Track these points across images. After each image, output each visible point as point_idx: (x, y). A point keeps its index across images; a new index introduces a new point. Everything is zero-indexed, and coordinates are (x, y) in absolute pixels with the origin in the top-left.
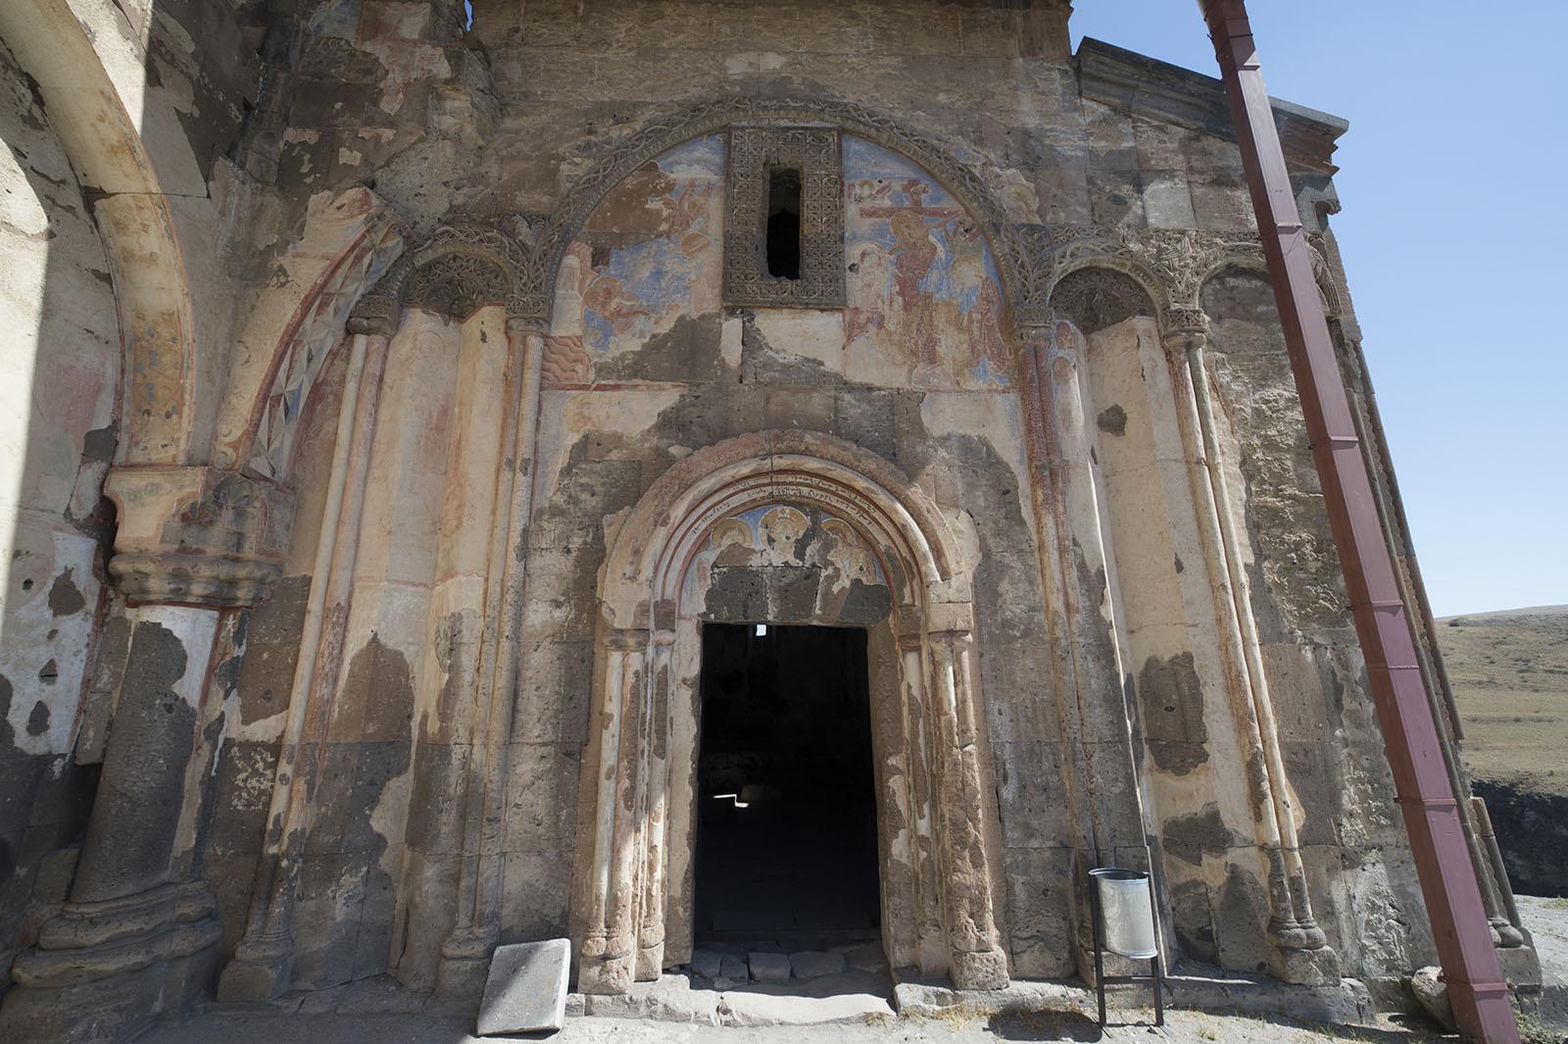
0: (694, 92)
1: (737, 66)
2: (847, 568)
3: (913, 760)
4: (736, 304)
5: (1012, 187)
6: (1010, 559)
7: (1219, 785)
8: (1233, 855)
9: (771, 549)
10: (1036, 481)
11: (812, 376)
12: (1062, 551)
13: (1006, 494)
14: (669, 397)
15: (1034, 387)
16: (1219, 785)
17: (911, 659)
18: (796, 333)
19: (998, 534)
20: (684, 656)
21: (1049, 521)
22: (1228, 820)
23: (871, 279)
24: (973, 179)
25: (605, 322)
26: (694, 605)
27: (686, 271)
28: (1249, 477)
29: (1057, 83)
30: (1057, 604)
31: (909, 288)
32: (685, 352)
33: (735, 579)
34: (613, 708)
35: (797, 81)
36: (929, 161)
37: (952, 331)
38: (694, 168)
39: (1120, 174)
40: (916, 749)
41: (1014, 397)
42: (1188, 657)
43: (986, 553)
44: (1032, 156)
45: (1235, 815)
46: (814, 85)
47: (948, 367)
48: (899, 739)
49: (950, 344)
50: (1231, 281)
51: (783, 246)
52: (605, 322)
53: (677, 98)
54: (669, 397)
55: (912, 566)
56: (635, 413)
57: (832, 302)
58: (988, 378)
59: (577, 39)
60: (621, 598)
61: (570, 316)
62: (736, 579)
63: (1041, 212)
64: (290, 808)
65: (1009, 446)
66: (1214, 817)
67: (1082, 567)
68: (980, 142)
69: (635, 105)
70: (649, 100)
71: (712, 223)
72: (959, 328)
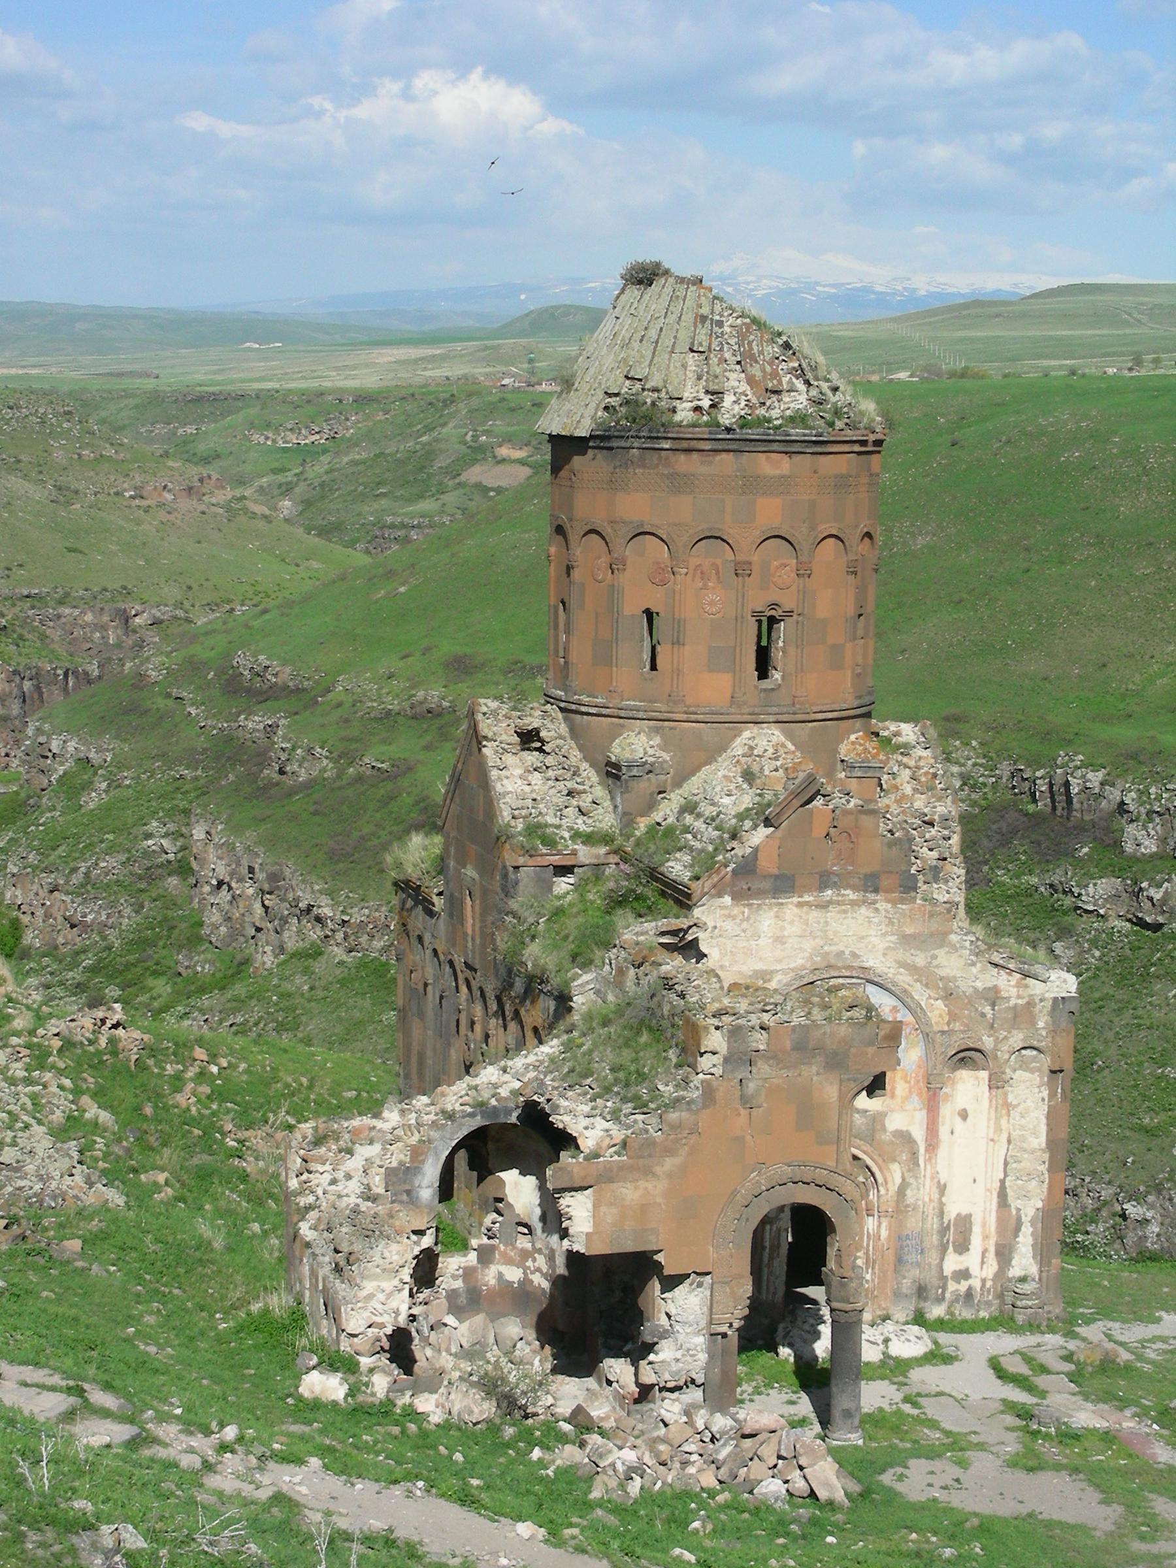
3: (867, 1253)
6: (912, 1181)
7: (971, 1260)
8: (971, 1281)
10: (927, 1150)
12: (932, 1178)
13: (914, 1154)
16: (971, 1260)
17: (871, 1218)
19: (909, 1171)
21: (928, 1167)
22: (971, 1271)
24: (922, 1008)
28: (1009, 1142)
30: (927, 1199)
34: (767, 1244)
35: (847, 953)
37: (902, 1082)
39: (987, 1000)
40: (868, 1250)
41: (924, 1112)
42: (971, 1215)
43: (903, 1180)
45: (975, 1270)
46: (855, 955)
47: (899, 1100)
48: (862, 1247)
50: (1023, 1052)
53: (791, 966)
59: (744, 931)
63: (948, 1024)
65: (919, 1134)
66: (967, 1270)
67: (939, 1182)
68: (927, 986)
69: (772, 972)
70: (779, 968)
72: (906, 1082)
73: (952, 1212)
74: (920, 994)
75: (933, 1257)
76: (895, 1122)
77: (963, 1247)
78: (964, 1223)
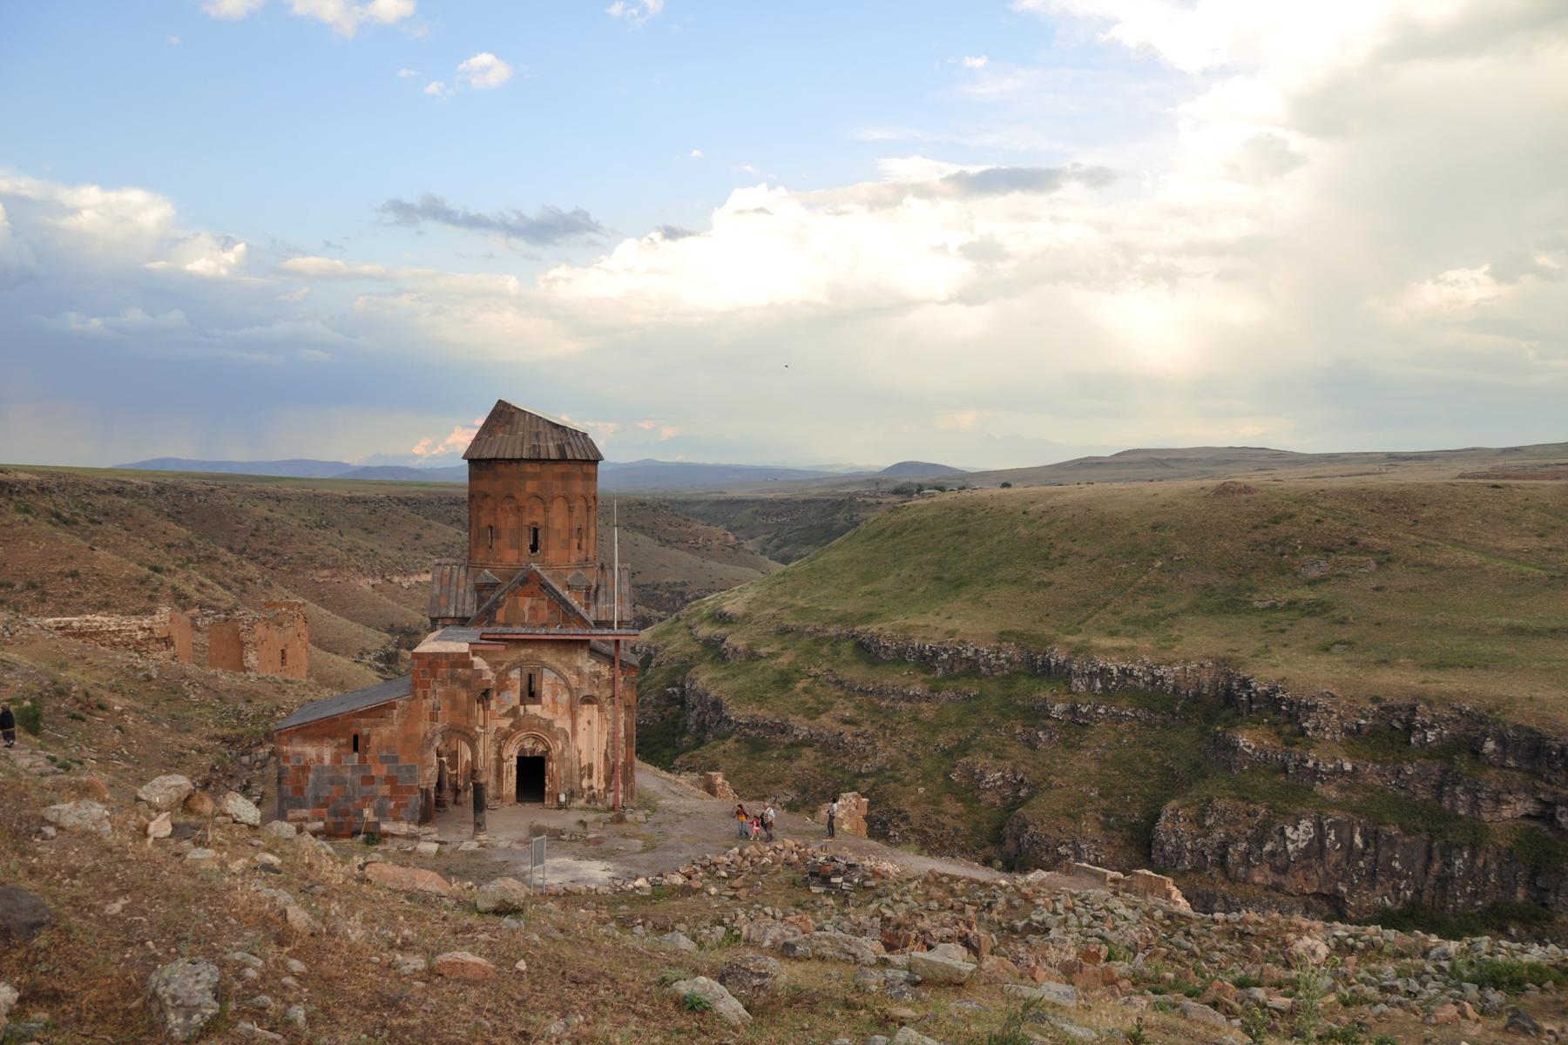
0: (514, 658)
1: (523, 652)
2: (541, 748)
4: (522, 703)
5: (574, 680)
7: (594, 781)
9: (528, 745)
11: (536, 716)
14: (511, 720)
15: (574, 717)
18: (533, 709)
20: (514, 762)
23: (546, 697)
25: (501, 706)
26: (516, 754)
27: (513, 697)
29: (586, 655)
31: (554, 700)
32: (514, 712)
33: (522, 750)
36: (559, 674)
38: (515, 675)
44: (579, 673)
49: (560, 711)
51: (531, 693)
52: (501, 706)
54: (511, 720)
55: (549, 749)
56: (506, 723)
57: (539, 702)
58: (567, 716)
60: (505, 756)
61: (493, 704)
62: (522, 750)
64: (461, 783)
65: (568, 729)
71: (518, 687)
73: (585, 762)
74: (567, 673)
75: (577, 780)
76: (558, 724)
77: (590, 777)
78: (590, 767)
